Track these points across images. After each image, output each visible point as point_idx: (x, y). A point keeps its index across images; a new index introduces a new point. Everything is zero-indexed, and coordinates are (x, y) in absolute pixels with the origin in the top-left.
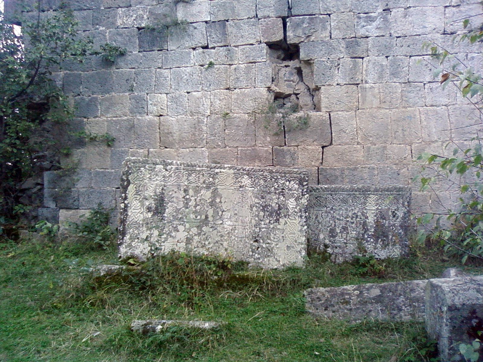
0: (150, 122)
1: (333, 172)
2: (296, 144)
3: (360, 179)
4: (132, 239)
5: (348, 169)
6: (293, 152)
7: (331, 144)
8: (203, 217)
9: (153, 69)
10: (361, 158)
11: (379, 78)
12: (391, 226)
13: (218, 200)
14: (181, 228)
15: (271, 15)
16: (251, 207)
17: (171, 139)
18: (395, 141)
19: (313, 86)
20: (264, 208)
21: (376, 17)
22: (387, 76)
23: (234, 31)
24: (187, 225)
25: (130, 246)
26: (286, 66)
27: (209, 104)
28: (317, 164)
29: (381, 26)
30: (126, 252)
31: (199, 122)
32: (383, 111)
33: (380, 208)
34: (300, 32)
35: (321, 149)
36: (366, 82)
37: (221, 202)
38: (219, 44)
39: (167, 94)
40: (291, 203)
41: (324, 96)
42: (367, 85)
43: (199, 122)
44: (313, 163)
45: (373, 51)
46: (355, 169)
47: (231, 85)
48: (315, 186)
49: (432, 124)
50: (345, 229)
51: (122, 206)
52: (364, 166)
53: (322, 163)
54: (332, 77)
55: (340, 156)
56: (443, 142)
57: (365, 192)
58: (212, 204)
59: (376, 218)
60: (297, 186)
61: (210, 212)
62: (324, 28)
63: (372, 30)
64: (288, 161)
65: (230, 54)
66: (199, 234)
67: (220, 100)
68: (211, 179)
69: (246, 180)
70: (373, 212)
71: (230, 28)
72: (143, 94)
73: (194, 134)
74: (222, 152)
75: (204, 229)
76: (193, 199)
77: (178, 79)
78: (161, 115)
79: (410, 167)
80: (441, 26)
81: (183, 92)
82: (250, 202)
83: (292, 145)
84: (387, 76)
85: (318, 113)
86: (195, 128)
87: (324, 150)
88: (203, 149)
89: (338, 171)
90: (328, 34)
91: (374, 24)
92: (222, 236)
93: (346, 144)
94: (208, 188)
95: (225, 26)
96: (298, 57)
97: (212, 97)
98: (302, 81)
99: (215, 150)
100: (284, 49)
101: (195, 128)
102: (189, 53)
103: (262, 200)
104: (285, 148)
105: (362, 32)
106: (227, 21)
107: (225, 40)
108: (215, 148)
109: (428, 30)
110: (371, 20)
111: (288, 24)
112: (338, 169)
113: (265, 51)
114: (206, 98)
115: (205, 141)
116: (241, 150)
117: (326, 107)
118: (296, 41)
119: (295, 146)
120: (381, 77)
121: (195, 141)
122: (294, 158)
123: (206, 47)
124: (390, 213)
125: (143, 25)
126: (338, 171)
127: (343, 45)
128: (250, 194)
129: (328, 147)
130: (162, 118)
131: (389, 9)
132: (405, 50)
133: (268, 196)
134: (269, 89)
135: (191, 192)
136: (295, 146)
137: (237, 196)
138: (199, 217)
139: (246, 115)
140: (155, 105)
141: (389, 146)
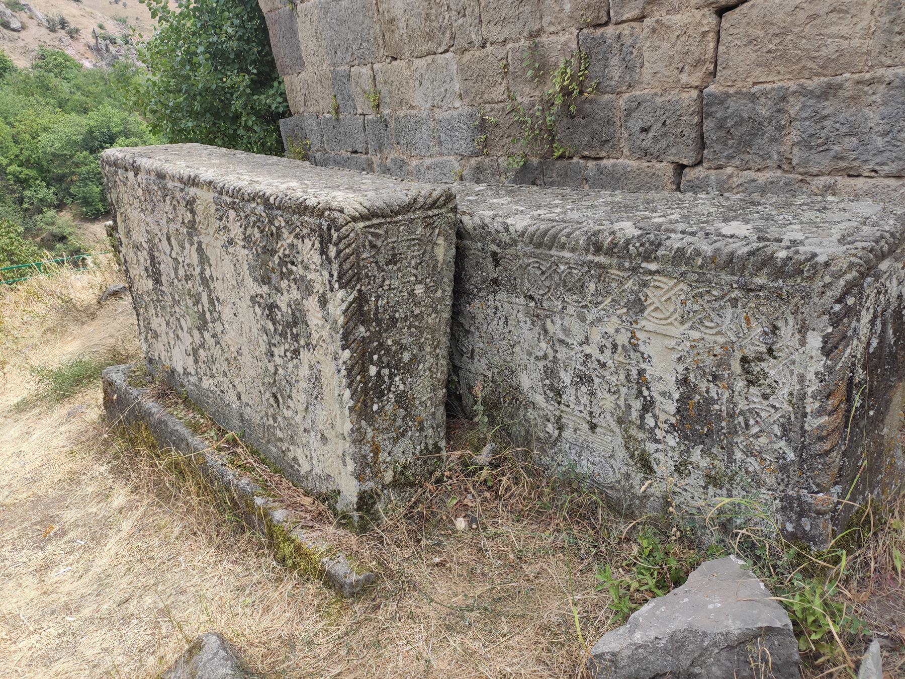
2: (636, 13)
3: (845, 130)
5: (802, 92)
6: (628, 41)
10: (856, 42)
12: (742, 413)
13: (207, 273)
17: (397, 34)
28: (695, 80)
33: (696, 335)
35: (711, 20)
44: (684, 78)
46: (829, 91)
52: (868, 76)
53: (714, 74)
55: (776, 40)
59: (681, 368)
70: (673, 343)
73: (428, 16)
83: (625, 18)
87: (725, 24)
88: (447, 55)
89: (763, 100)
99: (467, 57)
103: (266, 288)
104: (610, 30)
108: (466, 50)
112: (766, 93)
115: (448, 34)
116: (513, 49)
119: (634, 20)
121: (430, 37)
124: (736, 366)
126: (763, 100)
129: (737, 10)
136: (634, 20)
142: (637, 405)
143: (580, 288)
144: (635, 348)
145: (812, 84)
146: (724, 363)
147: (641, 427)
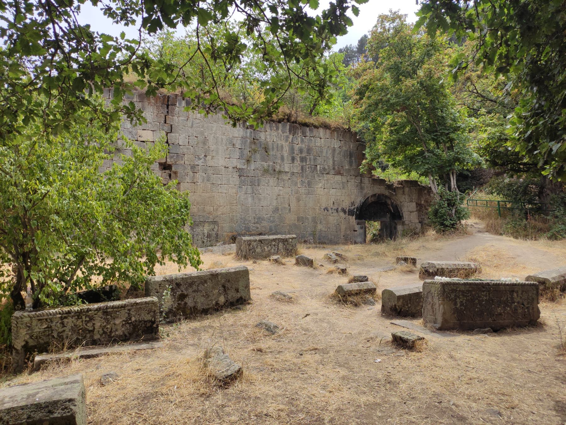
34: (172, 160)
54: (185, 179)
62: (182, 160)
80: (224, 165)
91: (201, 161)
105: (197, 163)
110: (200, 159)
118: (170, 163)
120: (203, 181)
127: (189, 167)
132: (212, 172)
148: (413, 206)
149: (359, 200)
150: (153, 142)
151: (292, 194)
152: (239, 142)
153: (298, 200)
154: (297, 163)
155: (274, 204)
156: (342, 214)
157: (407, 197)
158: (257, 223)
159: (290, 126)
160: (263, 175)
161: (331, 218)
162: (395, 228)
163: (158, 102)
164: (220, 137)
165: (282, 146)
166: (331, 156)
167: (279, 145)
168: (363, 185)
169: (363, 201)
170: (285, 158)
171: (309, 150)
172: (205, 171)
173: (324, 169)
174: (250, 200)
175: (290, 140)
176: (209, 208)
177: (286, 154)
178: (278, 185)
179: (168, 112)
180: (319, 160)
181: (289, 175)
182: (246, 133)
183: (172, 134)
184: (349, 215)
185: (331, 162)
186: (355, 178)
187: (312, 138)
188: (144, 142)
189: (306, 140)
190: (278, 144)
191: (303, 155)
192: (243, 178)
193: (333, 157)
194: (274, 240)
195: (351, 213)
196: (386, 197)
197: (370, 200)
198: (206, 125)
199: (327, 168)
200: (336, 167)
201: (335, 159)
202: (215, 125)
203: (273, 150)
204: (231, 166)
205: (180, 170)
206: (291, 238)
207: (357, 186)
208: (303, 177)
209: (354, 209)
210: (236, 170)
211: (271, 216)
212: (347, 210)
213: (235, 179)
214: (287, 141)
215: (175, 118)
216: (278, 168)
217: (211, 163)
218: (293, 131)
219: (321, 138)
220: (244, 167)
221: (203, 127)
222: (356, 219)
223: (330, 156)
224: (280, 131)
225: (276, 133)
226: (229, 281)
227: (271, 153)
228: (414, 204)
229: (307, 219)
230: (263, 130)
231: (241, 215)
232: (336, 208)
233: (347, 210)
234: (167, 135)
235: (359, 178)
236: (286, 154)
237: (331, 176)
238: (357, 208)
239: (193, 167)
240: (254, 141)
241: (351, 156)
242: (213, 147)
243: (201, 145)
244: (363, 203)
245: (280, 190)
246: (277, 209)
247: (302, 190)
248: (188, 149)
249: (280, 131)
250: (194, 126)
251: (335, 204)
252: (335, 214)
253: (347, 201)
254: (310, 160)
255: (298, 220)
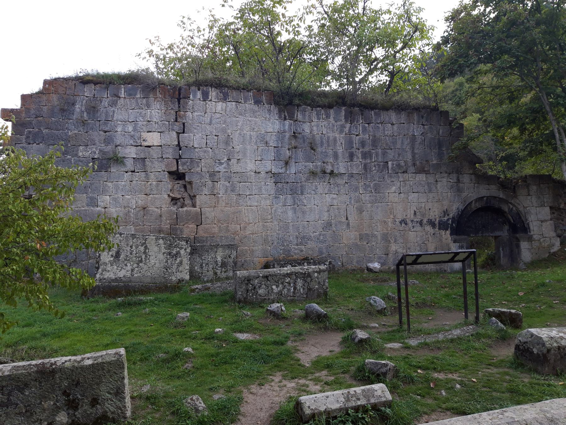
0: (99, 211)
1: (202, 238)
4: (103, 271)
5: (210, 237)
7: (201, 224)
8: (140, 259)
9: (102, 182)
11: (225, 192)
13: (147, 251)
14: (129, 265)
15: (170, 157)
16: (164, 253)
18: (233, 223)
19: (192, 195)
20: (170, 254)
21: (224, 163)
22: (229, 191)
23: (150, 164)
24: (132, 263)
25: (102, 274)
26: (178, 183)
27: (135, 202)
28: (194, 234)
29: (226, 167)
30: (100, 277)
31: (129, 212)
32: (227, 208)
34: (185, 167)
36: (219, 194)
37: (149, 252)
38: (141, 171)
39: (110, 196)
40: (182, 252)
41: (199, 200)
42: (220, 196)
43: (129, 212)
45: (223, 179)
46: (214, 237)
47: (148, 192)
48: (193, 244)
49: (250, 215)
50: (207, 264)
51: (98, 254)
53: (196, 234)
54: (202, 191)
56: (255, 223)
57: (217, 246)
58: (145, 253)
60: (185, 244)
61: (143, 257)
62: (198, 166)
63: (222, 168)
64: (179, 233)
65: (147, 177)
66: (138, 267)
67: (141, 200)
68: (144, 241)
69: (161, 241)
71: (148, 163)
72: (95, 195)
74: (142, 228)
75: (140, 264)
76: (135, 250)
77: (117, 188)
78: (106, 208)
79: (240, 235)
80: (254, 169)
81: (120, 195)
82: (163, 251)
84: (229, 191)
85: (195, 209)
86: (127, 215)
90: (200, 169)
91: (223, 166)
92: (149, 267)
93: (209, 224)
94: (142, 246)
95: (144, 161)
96: (184, 179)
97: (137, 199)
98: (186, 191)
99: (138, 227)
100: (177, 174)
101: (127, 215)
102: (124, 174)
104: (177, 226)
105: (217, 169)
106: (146, 158)
107: (145, 169)
109: (248, 170)
110: (221, 164)
111: (179, 163)
113: (167, 176)
114: (133, 199)
117: (199, 206)
118: (183, 171)
120: (226, 191)
121: (125, 222)
122: (182, 231)
123: (134, 172)
125: (96, 157)
127: (208, 175)
128: (163, 248)
130: (106, 209)
131: (230, 159)
132: (237, 179)
133: (172, 248)
134: (169, 196)
135: (134, 247)
137: (156, 249)
138: (138, 259)
139: (156, 209)
140: (102, 202)
141: (230, 225)
142: (215, 265)
143: (208, 251)
144: (216, 257)
145: (211, 236)
146: (227, 256)
147: (216, 268)
148: (546, 212)
149: (455, 208)
150: (161, 146)
151: (350, 202)
152: (274, 138)
153: (360, 211)
154: (358, 160)
155: (325, 218)
156: (428, 228)
157: (534, 199)
158: (301, 244)
159: (346, 111)
160: (308, 179)
161: (411, 235)
162: (518, 246)
163: (167, 96)
164: (248, 133)
165: (335, 140)
166: (408, 147)
167: (331, 138)
168: (461, 185)
169: (462, 207)
170: (340, 155)
171: (375, 142)
172: (229, 179)
173: (399, 166)
174: (290, 213)
175: (347, 130)
176: (233, 227)
177: (340, 150)
178: (330, 192)
179: (179, 107)
180: (391, 154)
181: (346, 178)
182: (284, 125)
183: (185, 134)
184: (439, 229)
185: (409, 157)
186: (448, 176)
187: (380, 125)
188: (149, 147)
189: (370, 128)
190: (328, 137)
191: (367, 149)
192: (280, 185)
193: (413, 148)
194: (288, 275)
195: (443, 226)
196: (501, 200)
197: (474, 207)
198: (229, 120)
199: (402, 164)
200: (418, 163)
201: (416, 151)
202: (241, 118)
203: (322, 146)
204: (263, 170)
205: (195, 180)
206: (316, 272)
207: (452, 187)
208: (366, 179)
209: (448, 220)
210: (270, 174)
211: (320, 235)
212: (437, 222)
213: (270, 186)
214: (341, 132)
215: (189, 114)
216: (329, 169)
217: (235, 167)
218: (350, 117)
219: (393, 124)
220: (281, 171)
221: (225, 122)
222: (451, 234)
223: (408, 148)
224: (332, 119)
225: (325, 123)
226: (78, 383)
227: (319, 150)
228: (547, 209)
229: (374, 236)
230: (307, 118)
231: (278, 234)
232: (419, 220)
233: (437, 222)
234: (178, 137)
235: (454, 176)
236: (340, 150)
237: (410, 175)
238: (453, 218)
239: (213, 175)
240: (295, 136)
241: (440, 145)
242: (237, 148)
243: (222, 146)
244: (463, 211)
245: (333, 199)
246: (328, 225)
247: (366, 197)
248: (205, 152)
249: (332, 119)
250: (214, 122)
251: (418, 214)
252: (418, 228)
253: (436, 210)
254: (377, 155)
255: (361, 239)
